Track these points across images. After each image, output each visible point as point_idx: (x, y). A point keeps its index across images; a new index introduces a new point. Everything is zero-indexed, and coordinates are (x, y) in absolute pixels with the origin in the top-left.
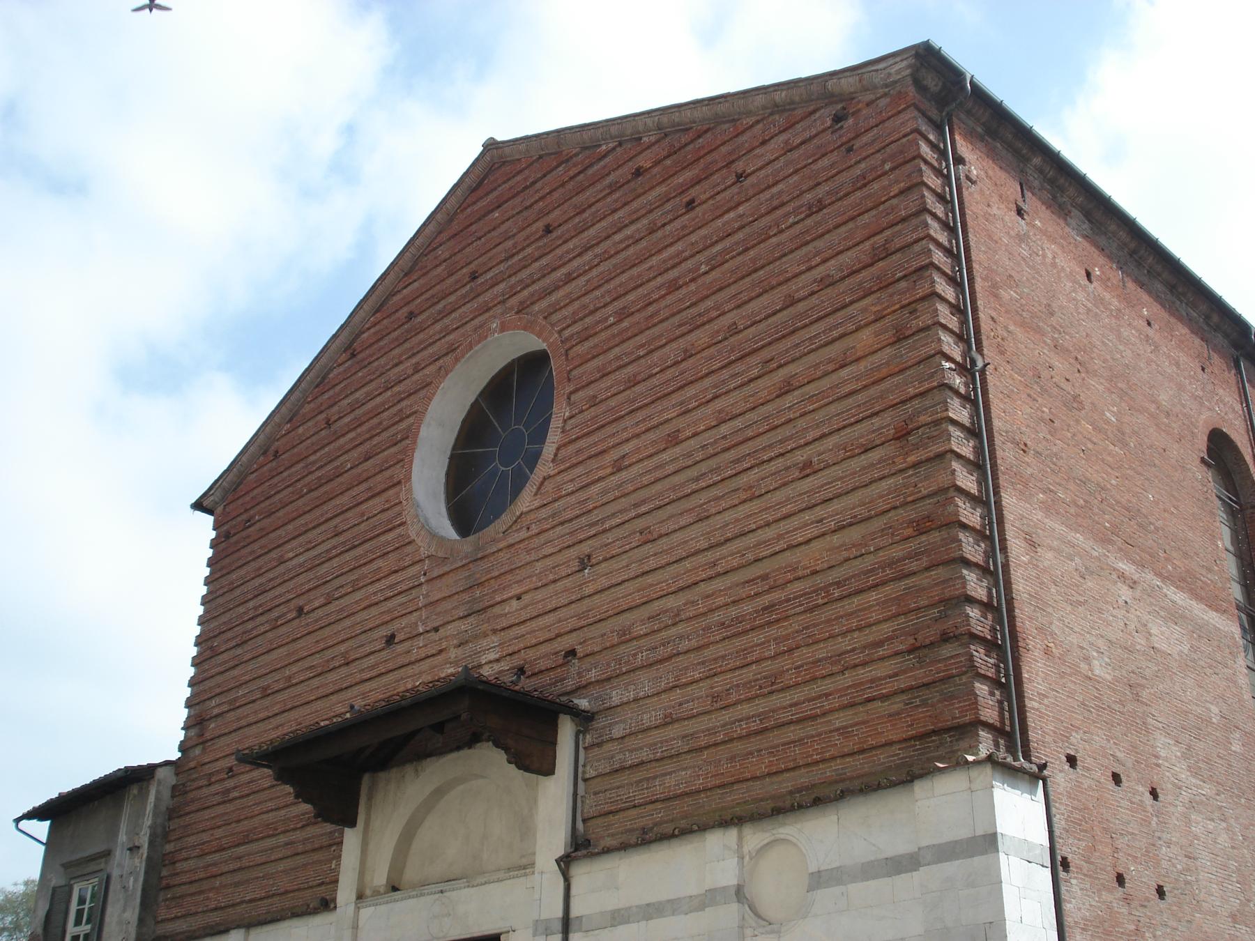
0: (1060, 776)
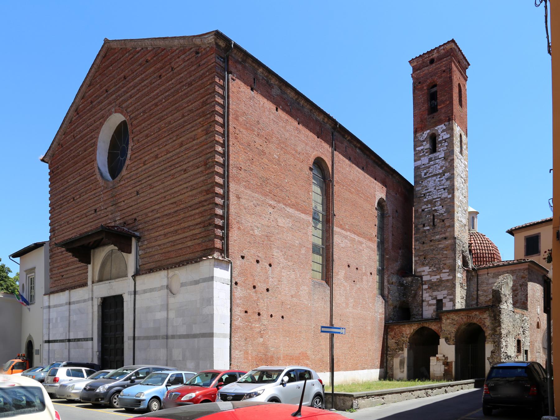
0: (238, 262)
